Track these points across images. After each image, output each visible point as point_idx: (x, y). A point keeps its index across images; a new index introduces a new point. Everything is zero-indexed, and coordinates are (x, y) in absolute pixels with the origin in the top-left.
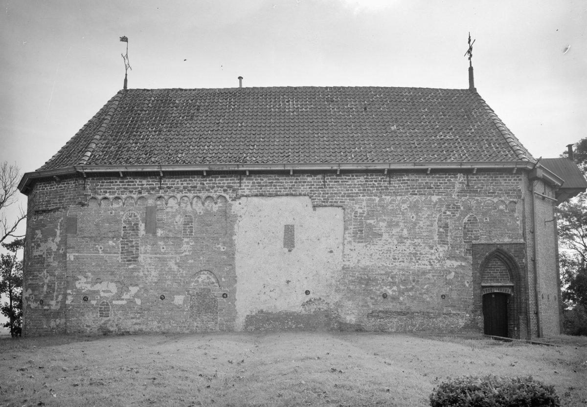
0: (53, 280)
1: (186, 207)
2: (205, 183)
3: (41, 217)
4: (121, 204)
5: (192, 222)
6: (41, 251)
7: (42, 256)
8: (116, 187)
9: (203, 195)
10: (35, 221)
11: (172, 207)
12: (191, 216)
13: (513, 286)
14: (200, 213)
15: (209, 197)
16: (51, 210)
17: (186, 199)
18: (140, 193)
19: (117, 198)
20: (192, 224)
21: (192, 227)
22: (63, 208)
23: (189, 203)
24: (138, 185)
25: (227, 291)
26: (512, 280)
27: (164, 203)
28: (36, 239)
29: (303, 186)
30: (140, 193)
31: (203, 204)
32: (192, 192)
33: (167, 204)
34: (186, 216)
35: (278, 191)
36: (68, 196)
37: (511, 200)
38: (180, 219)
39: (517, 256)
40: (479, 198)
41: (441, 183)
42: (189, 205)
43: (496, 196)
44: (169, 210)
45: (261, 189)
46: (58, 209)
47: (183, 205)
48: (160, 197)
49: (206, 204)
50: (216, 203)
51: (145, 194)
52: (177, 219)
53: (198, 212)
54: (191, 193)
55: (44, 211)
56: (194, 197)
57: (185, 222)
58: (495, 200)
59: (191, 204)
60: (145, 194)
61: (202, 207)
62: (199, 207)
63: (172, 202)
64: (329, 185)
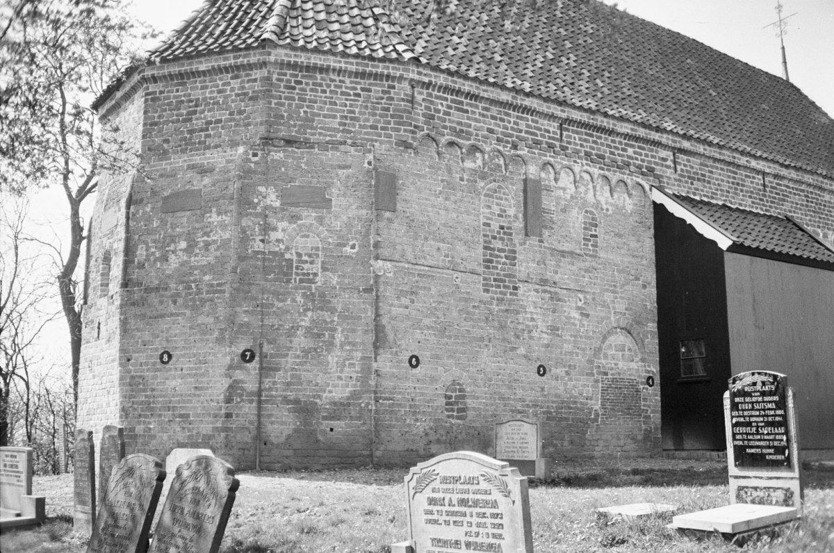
0: (328, 320)
2: (616, 152)
3: (278, 155)
4: (479, 162)
5: (596, 226)
6: (278, 241)
7: (282, 255)
8: (473, 124)
9: (615, 177)
10: (255, 163)
11: (564, 189)
12: (594, 214)
14: (607, 210)
20: (595, 231)
21: (596, 236)
23: (590, 186)
24: (512, 129)
27: (552, 176)
28: (259, 209)
30: (515, 147)
31: (611, 191)
32: (598, 166)
33: (556, 180)
34: (586, 212)
36: (368, 120)
38: (576, 219)
42: (592, 190)
44: (561, 193)
46: (335, 145)
48: (546, 164)
49: (616, 196)
50: (630, 195)
51: (524, 152)
52: (574, 212)
54: (595, 167)
55: (289, 142)
57: (585, 223)
60: (524, 152)
61: (610, 200)
62: (604, 196)
63: (566, 180)
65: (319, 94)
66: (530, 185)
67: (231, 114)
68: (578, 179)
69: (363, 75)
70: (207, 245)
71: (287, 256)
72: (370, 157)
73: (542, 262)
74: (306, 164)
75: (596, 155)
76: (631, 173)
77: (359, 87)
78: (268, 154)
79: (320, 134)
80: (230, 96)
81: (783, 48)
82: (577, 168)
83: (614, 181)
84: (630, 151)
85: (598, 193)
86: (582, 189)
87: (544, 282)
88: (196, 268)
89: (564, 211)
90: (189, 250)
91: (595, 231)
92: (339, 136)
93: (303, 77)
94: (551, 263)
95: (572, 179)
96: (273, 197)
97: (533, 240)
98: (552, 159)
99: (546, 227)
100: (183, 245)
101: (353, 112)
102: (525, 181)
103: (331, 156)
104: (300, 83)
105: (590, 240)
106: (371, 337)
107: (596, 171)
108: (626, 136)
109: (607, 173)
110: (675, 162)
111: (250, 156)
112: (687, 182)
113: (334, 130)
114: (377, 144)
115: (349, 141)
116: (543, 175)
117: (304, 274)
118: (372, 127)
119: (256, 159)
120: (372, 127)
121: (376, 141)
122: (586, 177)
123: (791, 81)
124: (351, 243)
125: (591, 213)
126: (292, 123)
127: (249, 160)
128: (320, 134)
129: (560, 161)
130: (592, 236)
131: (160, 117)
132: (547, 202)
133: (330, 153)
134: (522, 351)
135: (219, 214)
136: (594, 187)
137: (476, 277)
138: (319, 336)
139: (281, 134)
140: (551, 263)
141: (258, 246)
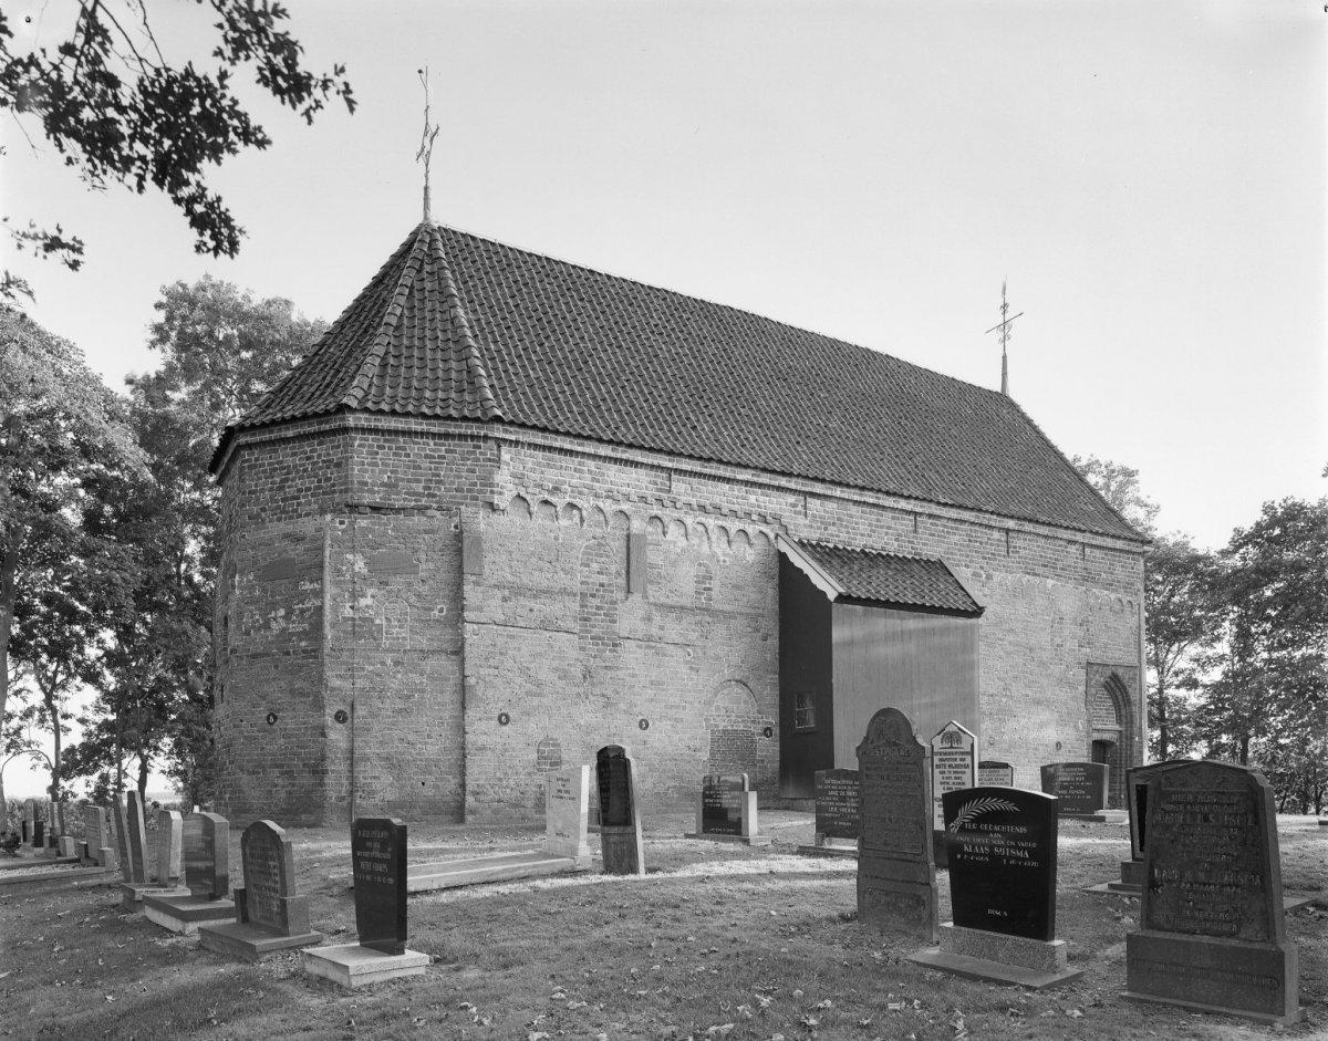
3: (363, 523)
10: (343, 531)
13: (1120, 731)
16: (398, 511)
20: (710, 584)
21: (709, 589)
22: (440, 509)
23: (705, 538)
25: (771, 723)
26: (1119, 721)
27: (660, 530)
29: (887, 534)
33: (664, 533)
34: (700, 565)
35: (852, 539)
43: (1113, 590)
45: (826, 529)
46: (422, 510)
50: (751, 545)
53: (722, 558)
55: (375, 509)
57: (697, 576)
63: (674, 531)
65: (403, 458)
66: (633, 540)
67: (319, 481)
68: (690, 531)
69: (447, 436)
70: (302, 611)
71: (378, 622)
72: (457, 519)
73: (649, 619)
74: (393, 530)
75: (711, 505)
77: (443, 448)
78: (355, 522)
79: (405, 499)
80: (317, 463)
81: (1004, 357)
82: (689, 521)
83: (733, 532)
84: (752, 499)
85: (714, 545)
86: (695, 541)
87: (650, 639)
88: (292, 634)
89: (674, 564)
90: (287, 617)
91: (710, 584)
92: (424, 501)
93: (386, 441)
94: (657, 618)
95: (683, 531)
96: (361, 564)
97: (636, 598)
98: (660, 512)
99: (651, 582)
100: (282, 612)
101: (439, 475)
102: (628, 536)
103: (417, 520)
104: (384, 447)
105: (703, 593)
106: (456, 697)
107: (711, 522)
108: (746, 483)
109: (724, 524)
110: (805, 507)
111: (337, 524)
112: (818, 528)
113: (419, 494)
114: (463, 507)
115: (434, 505)
116: (650, 529)
117: (394, 639)
118: (457, 490)
119: (343, 526)
120: (457, 490)
121: (462, 504)
122: (701, 528)
123: (1014, 394)
124: (439, 607)
126: (376, 489)
127: (335, 528)
128: (405, 499)
129: (668, 514)
130: (705, 589)
131: (256, 485)
132: (653, 556)
133: (416, 518)
134: (622, 706)
135: (311, 582)
136: (709, 538)
137: (572, 636)
138: (409, 697)
139: (365, 502)
140: (657, 618)
141: (348, 612)
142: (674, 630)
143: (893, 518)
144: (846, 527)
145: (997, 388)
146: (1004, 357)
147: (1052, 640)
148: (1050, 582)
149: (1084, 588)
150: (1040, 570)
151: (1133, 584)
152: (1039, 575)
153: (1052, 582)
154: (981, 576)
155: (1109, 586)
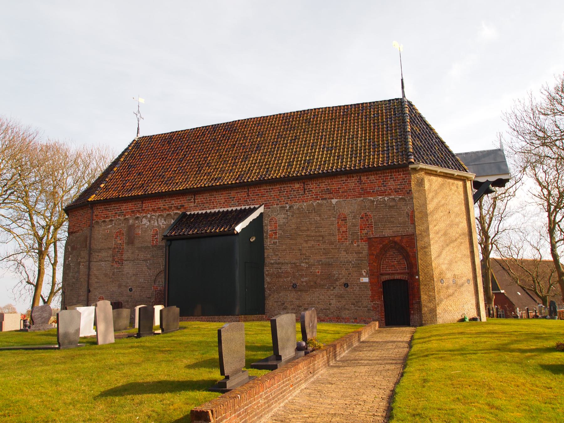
1: (154, 223)
15: (168, 215)
17: (154, 217)
18: (125, 216)
19: (111, 221)
29: (233, 200)
37: (401, 197)
39: (408, 247)
40: (372, 198)
41: (340, 188)
43: (386, 195)
47: (152, 222)
48: (138, 217)
56: (159, 215)
58: (386, 199)
59: (157, 220)
61: (165, 223)
63: (145, 221)
64: (251, 198)
76: (173, 210)
110: (194, 199)
123: (408, 97)
125: (156, 230)
142: (142, 256)
143: (236, 193)
144: (213, 202)
145: (400, 96)
146: (402, 80)
147: (339, 230)
148: (334, 201)
149: (362, 199)
150: (327, 196)
151: (404, 188)
152: (326, 199)
153: (336, 200)
154: (286, 207)
155: (383, 193)
